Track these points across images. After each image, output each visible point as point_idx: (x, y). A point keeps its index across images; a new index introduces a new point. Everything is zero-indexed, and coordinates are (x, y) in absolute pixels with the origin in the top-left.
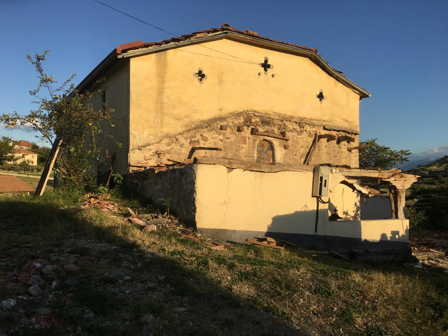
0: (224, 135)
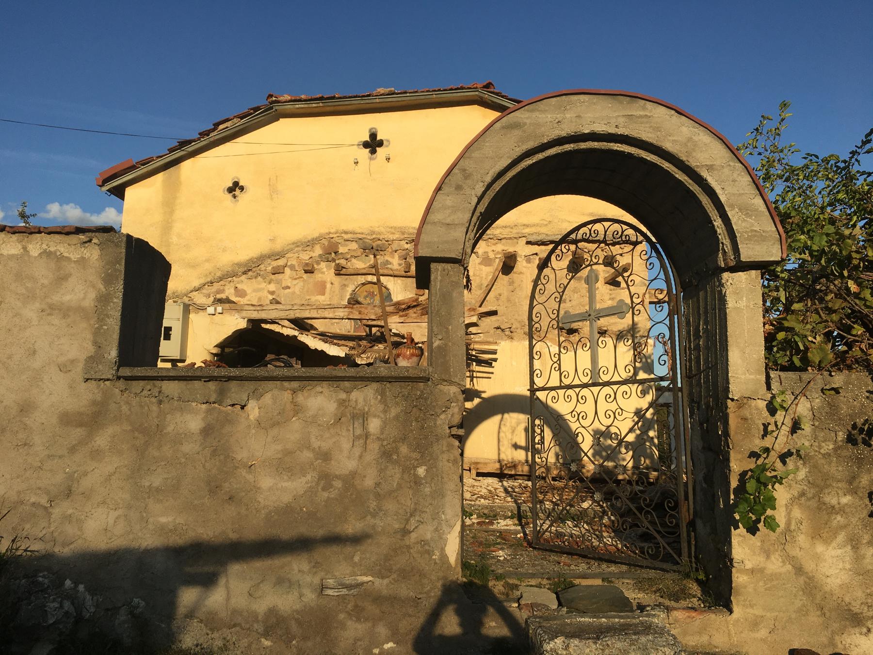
0: (278, 282)
